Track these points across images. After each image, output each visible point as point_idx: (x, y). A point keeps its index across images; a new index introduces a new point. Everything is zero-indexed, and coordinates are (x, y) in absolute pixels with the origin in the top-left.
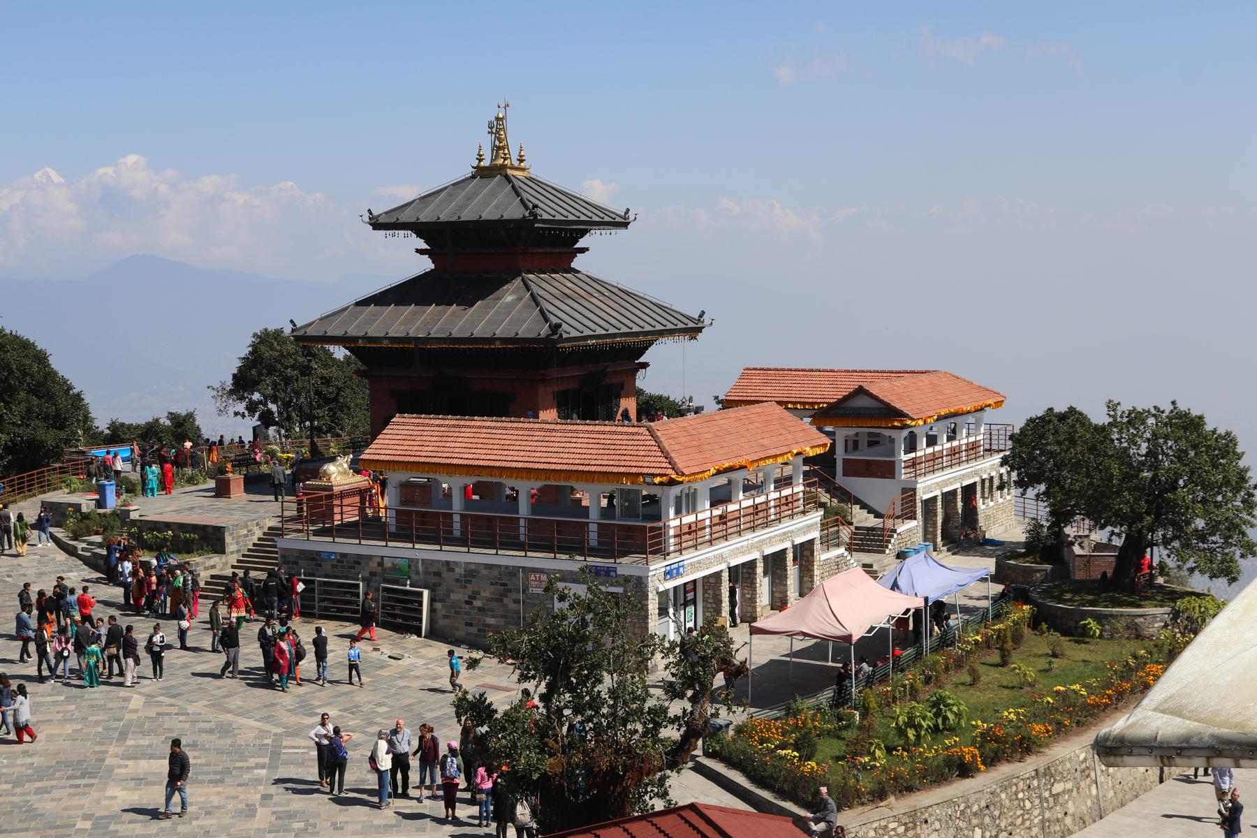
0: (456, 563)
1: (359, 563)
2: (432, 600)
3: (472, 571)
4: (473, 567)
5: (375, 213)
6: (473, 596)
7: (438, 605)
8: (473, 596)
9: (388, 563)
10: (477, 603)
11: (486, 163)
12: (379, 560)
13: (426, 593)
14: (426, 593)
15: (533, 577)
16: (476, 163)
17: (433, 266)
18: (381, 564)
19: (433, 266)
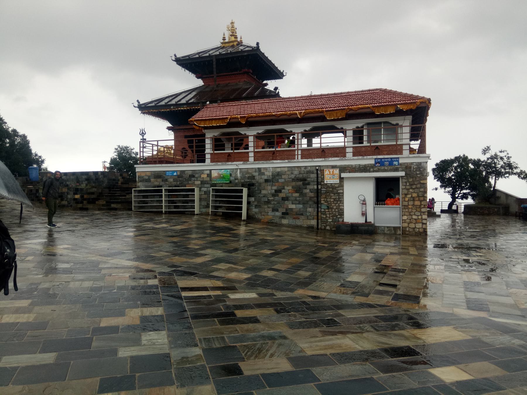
0: (266, 169)
1: (194, 176)
2: (249, 196)
3: (279, 172)
4: (279, 170)
5: (178, 56)
6: (278, 191)
7: (252, 199)
8: (278, 191)
9: (214, 174)
10: (281, 195)
11: (227, 40)
12: (208, 172)
13: (245, 191)
14: (245, 191)
15: (326, 172)
16: (222, 41)
17: (203, 84)
18: (209, 175)
19: (203, 84)
